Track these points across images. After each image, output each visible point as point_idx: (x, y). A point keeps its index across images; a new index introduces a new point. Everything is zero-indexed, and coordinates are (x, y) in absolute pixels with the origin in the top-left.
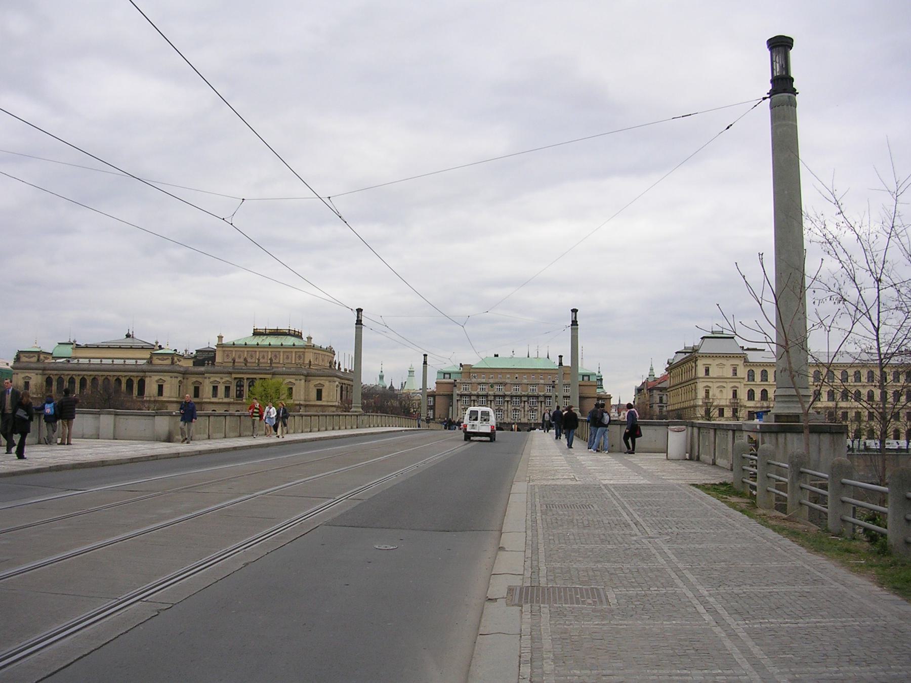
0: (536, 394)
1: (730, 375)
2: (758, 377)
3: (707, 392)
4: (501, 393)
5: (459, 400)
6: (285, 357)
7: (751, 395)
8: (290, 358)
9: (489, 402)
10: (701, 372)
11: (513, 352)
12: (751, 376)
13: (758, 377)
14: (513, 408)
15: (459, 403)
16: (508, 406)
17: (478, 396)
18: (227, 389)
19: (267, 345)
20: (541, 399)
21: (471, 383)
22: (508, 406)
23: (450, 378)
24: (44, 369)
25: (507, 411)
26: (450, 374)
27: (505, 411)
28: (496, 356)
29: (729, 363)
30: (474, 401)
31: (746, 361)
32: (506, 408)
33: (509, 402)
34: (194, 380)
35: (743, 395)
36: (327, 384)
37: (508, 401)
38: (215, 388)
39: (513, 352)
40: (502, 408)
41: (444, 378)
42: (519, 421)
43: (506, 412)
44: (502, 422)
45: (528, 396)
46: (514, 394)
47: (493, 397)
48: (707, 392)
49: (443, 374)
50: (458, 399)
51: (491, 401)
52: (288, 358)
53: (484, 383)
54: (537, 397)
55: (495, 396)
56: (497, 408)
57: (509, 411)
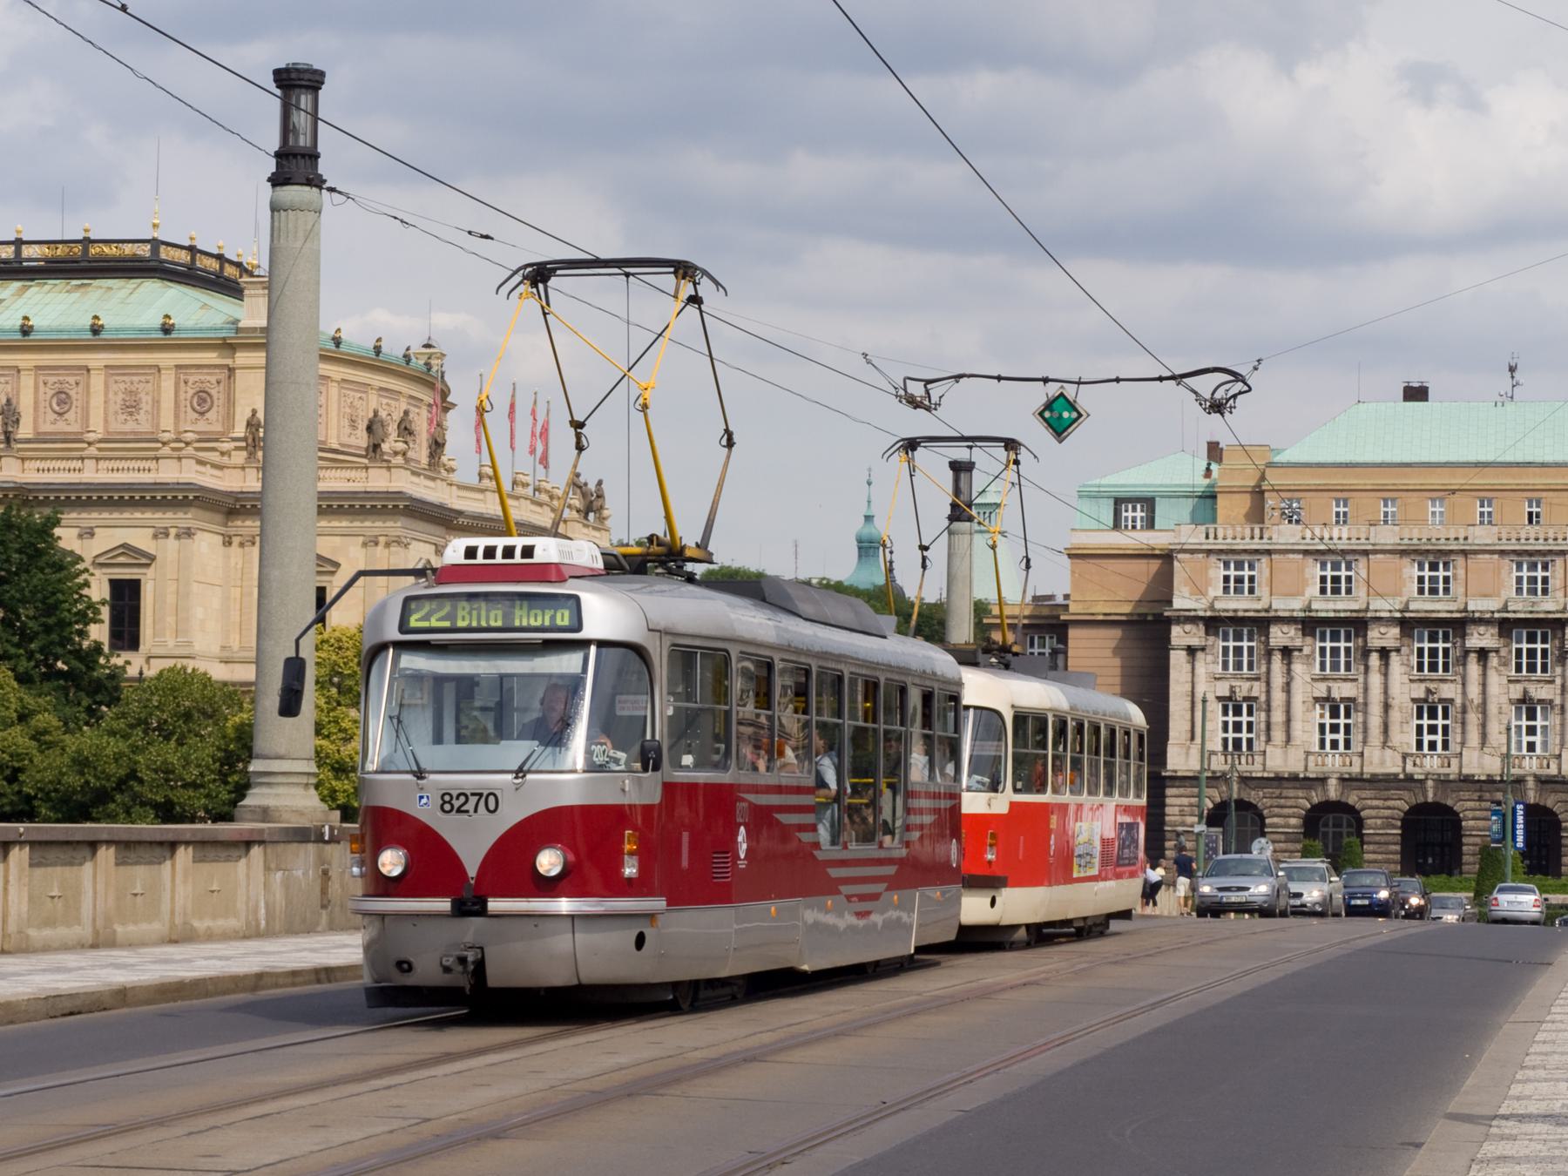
4: (1441, 607)
5: (1203, 649)
6: (116, 405)
8: (146, 406)
9: (1374, 660)
11: (1512, 369)
14: (1516, 692)
15: (1201, 669)
16: (1484, 685)
19: (10, 331)
21: (1269, 552)
22: (1484, 685)
23: (1150, 524)
25: (1483, 708)
26: (1149, 503)
27: (1464, 711)
28: (1416, 394)
30: (1287, 652)
32: (1474, 691)
33: (1494, 660)
37: (1483, 654)
39: (1512, 369)
40: (1448, 691)
41: (1117, 526)
42: (1553, 770)
43: (1473, 718)
44: (1453, 770)
46: (1521, 607)
47: (1396, 631)
49: (1112, 502)
50: (1195, 642)
51: (1384, 653)
52: (131, 408)
53: (1344, 552)
55: (1408, 625)
56: (1419, 691)
57: (1492, 708)
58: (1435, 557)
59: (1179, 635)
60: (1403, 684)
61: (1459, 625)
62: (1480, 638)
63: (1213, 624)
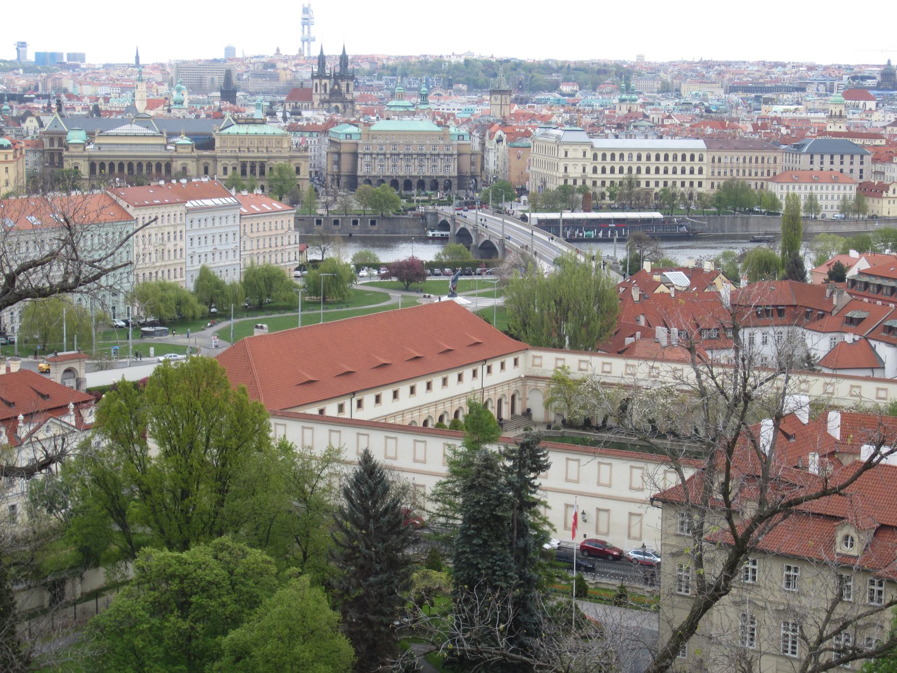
0: (423, 152)
1: (581, 156)
2: (600, 158)
3: (566, 168)
4: (396, 152)
7: (595, 170)
10: (562, 155)
12: (595, 157)
13: (600, 158)
17: (378, 154)
18: (234, 168)
20: (428, 156)
24: (90, 157)
29: (581, 149)
31: (592, 147)
34: (204, 161)
35: (589, 170)
36: (303, 163)
38: (225, 169)
45: (418, 154)
46: (406, 152)
48: (566, 168)
54: (425, 155)
55: (391, 154)
58: (395, 145)
59: (360, 156)
60: (390, 163)
61: (398, 155)
62: (401, 156)
63: (365, 154)
